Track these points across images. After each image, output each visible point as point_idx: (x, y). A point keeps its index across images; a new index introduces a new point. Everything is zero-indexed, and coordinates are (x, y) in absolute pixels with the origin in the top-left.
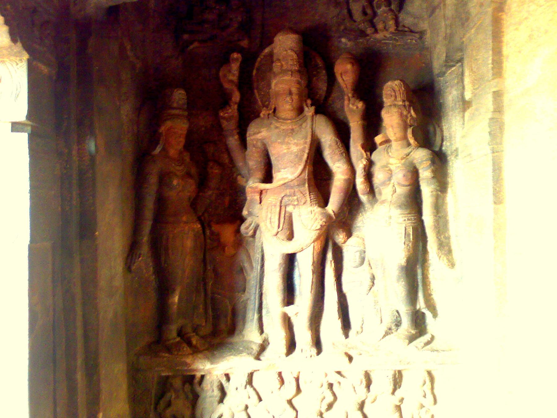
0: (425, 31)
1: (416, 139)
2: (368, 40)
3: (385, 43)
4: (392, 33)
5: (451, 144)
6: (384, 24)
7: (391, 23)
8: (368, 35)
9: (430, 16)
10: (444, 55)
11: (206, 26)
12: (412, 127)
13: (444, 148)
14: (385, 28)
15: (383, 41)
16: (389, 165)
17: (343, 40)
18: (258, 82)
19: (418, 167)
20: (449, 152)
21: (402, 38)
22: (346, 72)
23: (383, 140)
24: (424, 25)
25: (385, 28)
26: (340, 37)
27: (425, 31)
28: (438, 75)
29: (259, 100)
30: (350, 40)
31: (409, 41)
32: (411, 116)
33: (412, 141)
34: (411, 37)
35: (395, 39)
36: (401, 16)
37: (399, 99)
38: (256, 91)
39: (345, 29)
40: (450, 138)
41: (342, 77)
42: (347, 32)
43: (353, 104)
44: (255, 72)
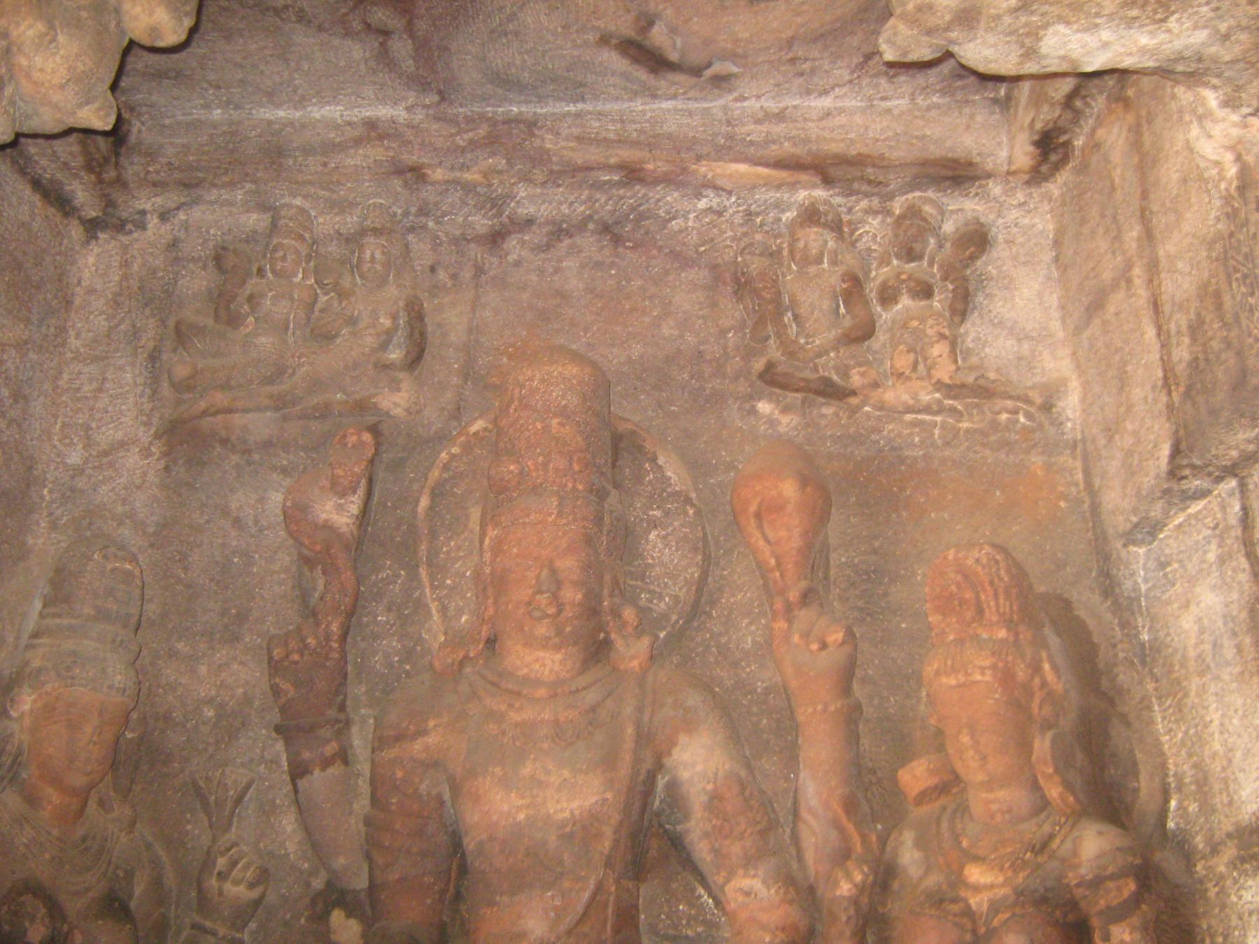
0: (1064, 382)
1: (1068, 786)
2: (854, 411)
3: (914, 424)
4: (939, 386)
5: (1207, 808)
6: (912, 356)
7: (939, 350)
8: (853, 393)
9: (1078, 331)
10: (1165, 450)
11: (263, 340)
12: (1049, 735)
13: (1171, 825)
14: (915, 368)
15: (909, 417)
16: (963, 894)
17: (764, 407)
18: (433, 535)
19: (1082, 904)
20: (1199, 842)
21: (977, 406)
22: (778, 507)
23: (934, 781)
24: (1056, 364)
25: (915, 368)
26: (752, 397)
27: (1064, 382)
28: (1129, 539)
29: (434, 607)
30: (785, 410)
31: (1004, 416)
32: (1044, 684)
33: (1054, 792)
34: (1009, 404)
35: (953, 410)
36: (972, 330)
37: (991, 615)
38: (423, 572)
39: (770, 366)
40: (1202, 782)
41: (760, 527)
42: (772, 379)
43: (806, 635)
44: (424, 502)
